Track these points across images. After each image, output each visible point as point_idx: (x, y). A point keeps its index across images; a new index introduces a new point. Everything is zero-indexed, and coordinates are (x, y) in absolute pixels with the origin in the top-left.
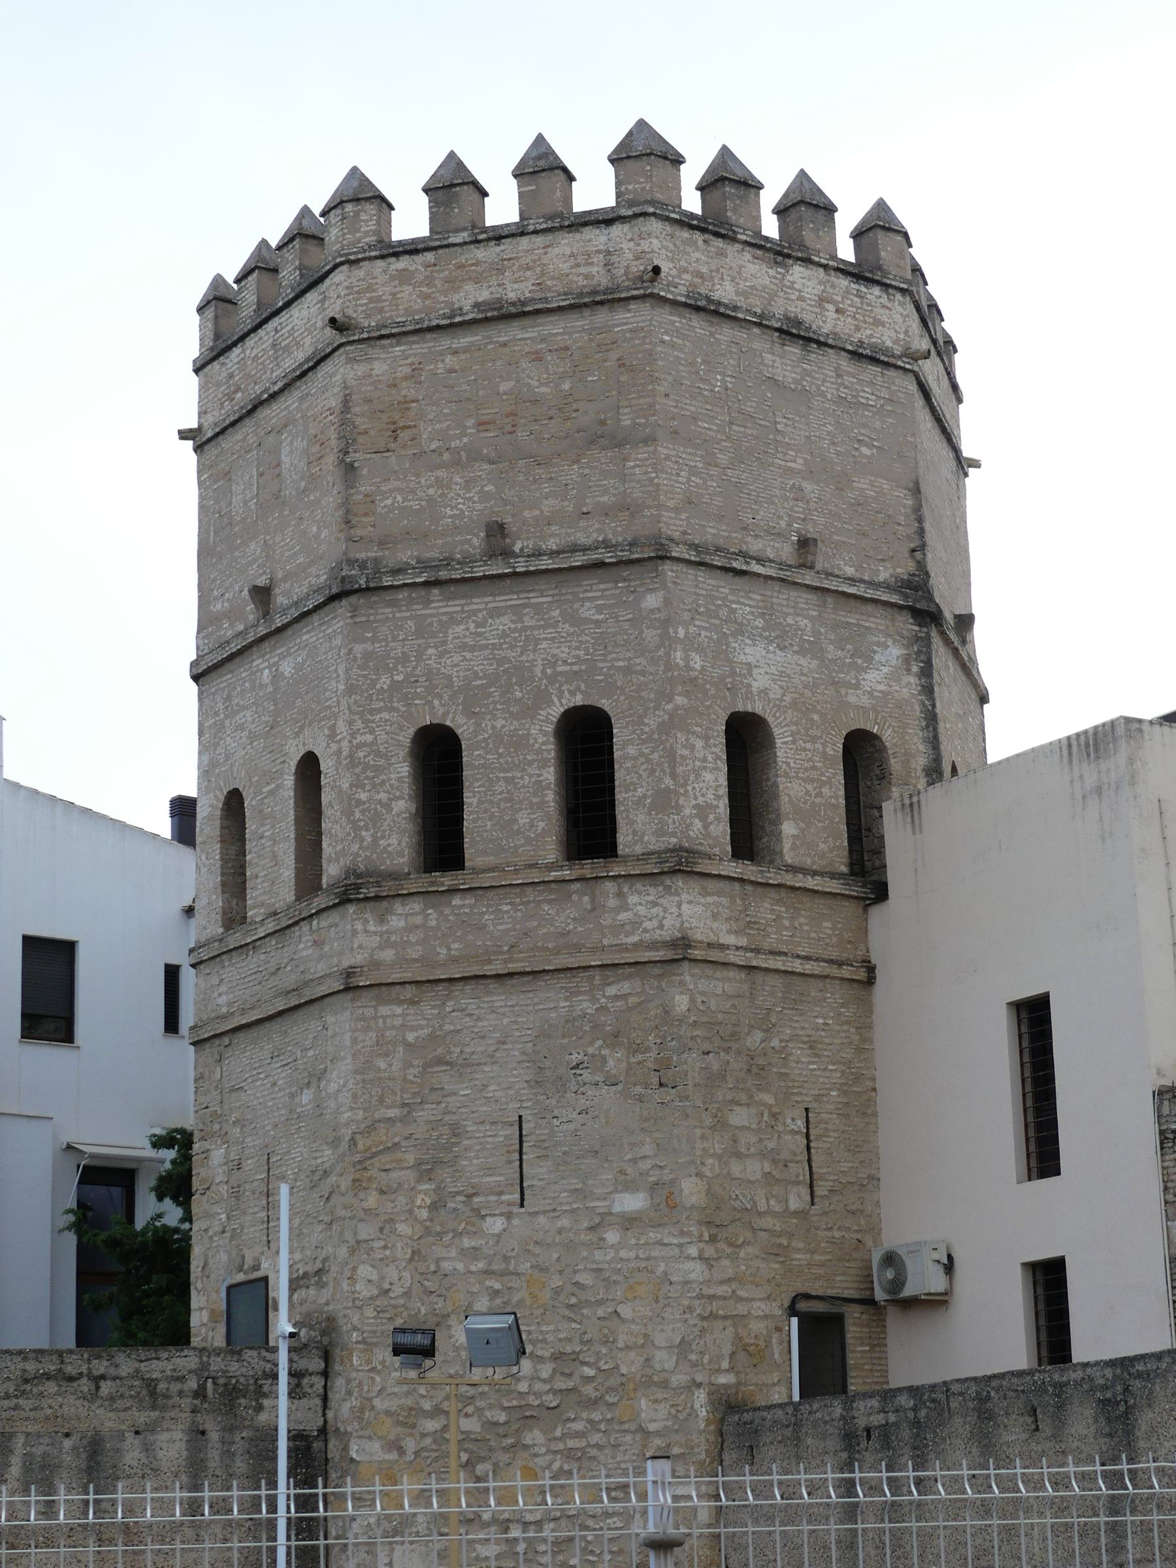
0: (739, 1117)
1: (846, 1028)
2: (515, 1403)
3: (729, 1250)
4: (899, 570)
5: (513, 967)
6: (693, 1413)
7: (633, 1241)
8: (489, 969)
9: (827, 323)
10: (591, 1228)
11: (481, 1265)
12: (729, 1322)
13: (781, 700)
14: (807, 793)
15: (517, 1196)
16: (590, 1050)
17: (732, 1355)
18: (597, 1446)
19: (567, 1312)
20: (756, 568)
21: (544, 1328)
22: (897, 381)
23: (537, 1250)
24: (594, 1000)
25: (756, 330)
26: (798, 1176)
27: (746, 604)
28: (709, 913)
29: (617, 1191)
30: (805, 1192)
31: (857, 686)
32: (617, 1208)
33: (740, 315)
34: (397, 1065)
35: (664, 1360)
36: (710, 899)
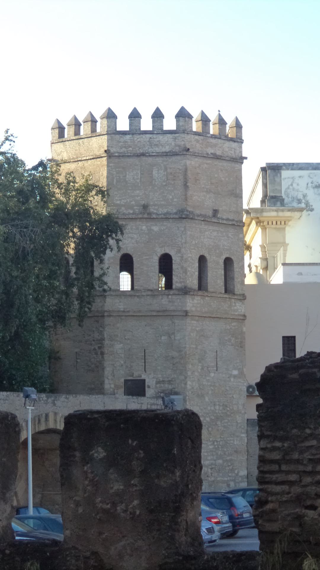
5: (217, 316)
11: (209, 384)
32: (233, 374)
35: (241, 407)
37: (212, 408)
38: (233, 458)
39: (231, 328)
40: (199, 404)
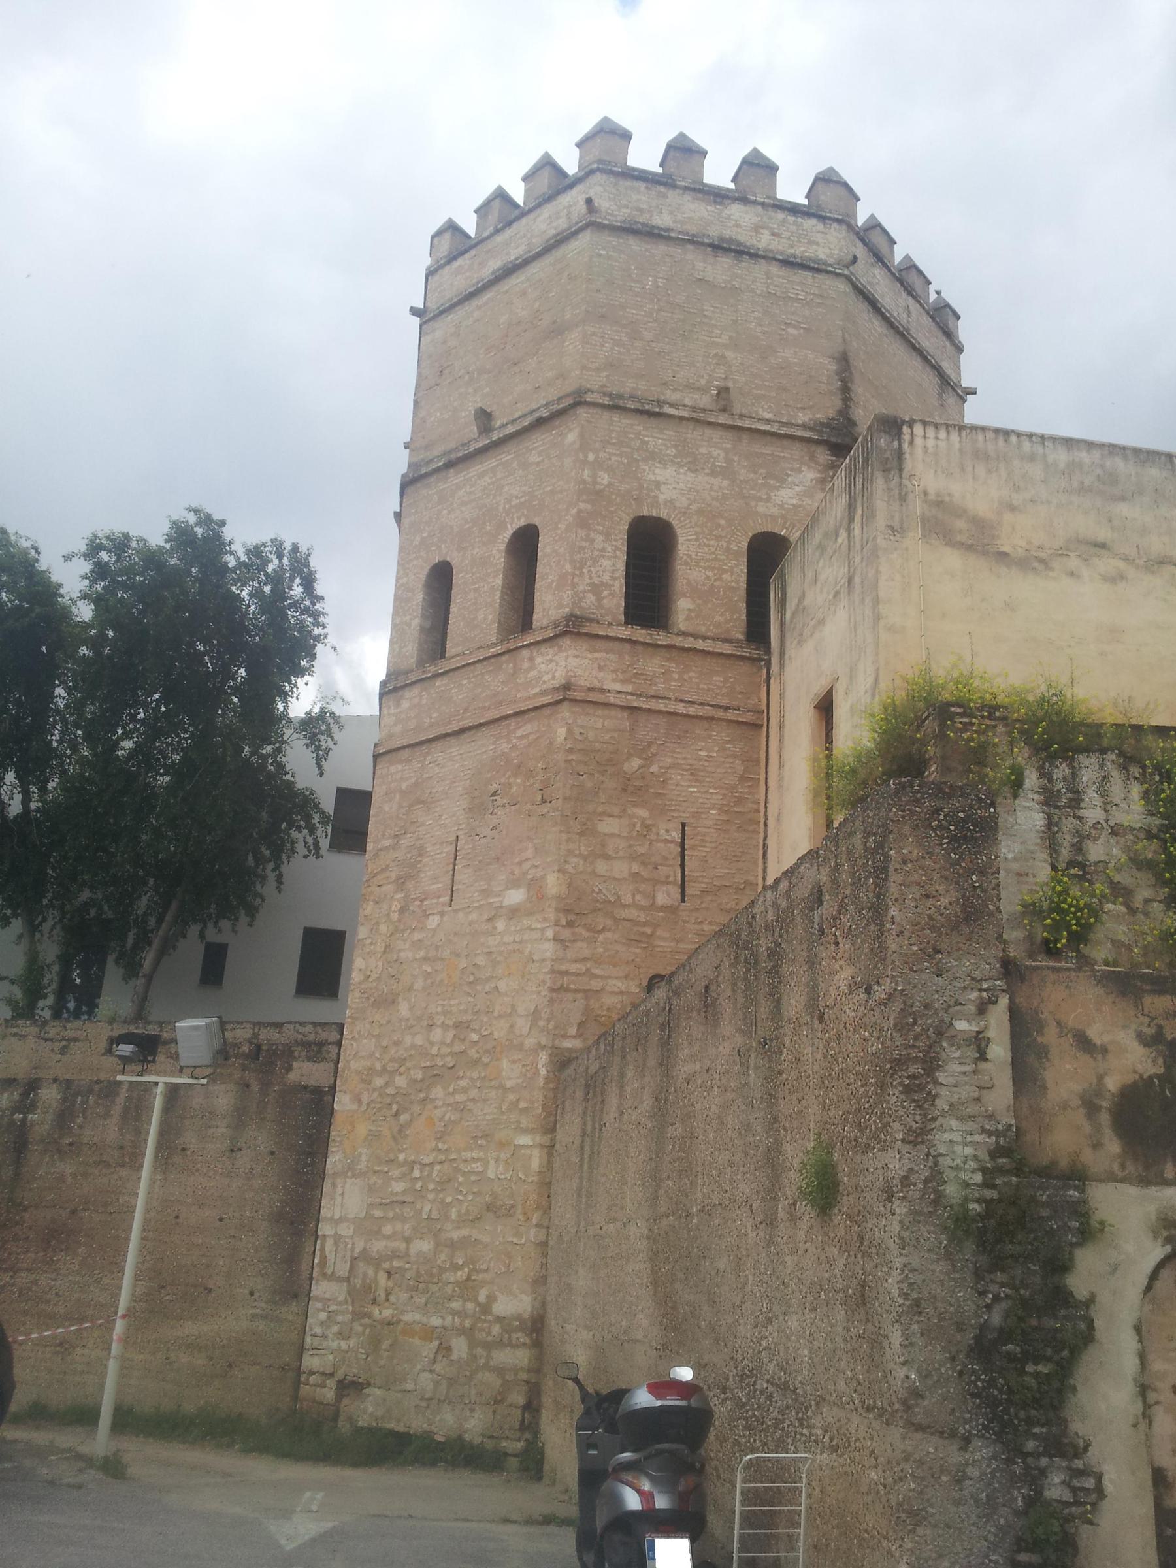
0: (608, 826)
1: (730, 760)
2: (428, 1064)
3: (586, 934)
4: (818, 416)
6: (537, 1072)
7: (513, 928)
9: (764, 241)
10: (490, 920)
11: (422, 954)
12: (580, 995)
13: (688, 508)
14: (708, 578)
15: (448, 898)
16: (503, 781)
17: (581, 1025)
18: (473, 1099)
20: (667, 410)
21: (452, 1002)
22: (828, 282)
24: (509, 741)
25: (690, 247)
26: (668, 877)
27: (657, 438)
28: (595, 665)
29: (507, 889)
30: (675, 892)
31: (768, 500)
32: (506, 903)
33: (673, 235)
35: (522, 1025)
36: (596, 655)
37: (419, 1040)
38: (475, 1235)
39: (514, 747)
40: (377, 1032)
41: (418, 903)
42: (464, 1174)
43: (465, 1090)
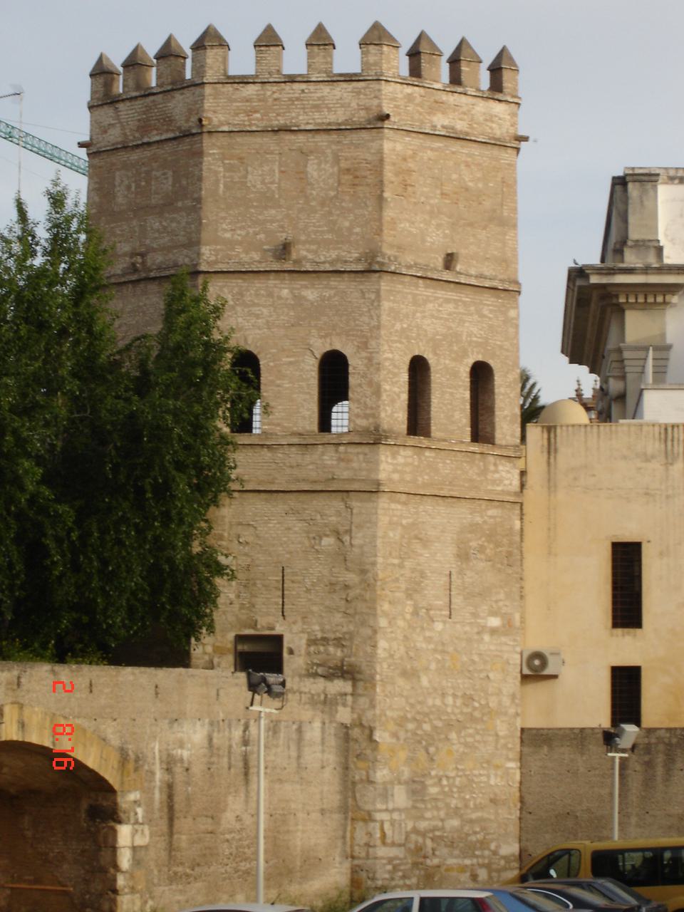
8: (442, 493)
10: (478, 633)
11: (432, 646)
16: (480, 543)
18: (478, 742)
19: (467, 674)
23: (456, 641)
24: (482, 517)
34: (397, 537)
35: (506, 701)
37: (438, 702)
38: (486, 815)
39: (485, 522)
40: (405, 693)
41: (424, 610)
42: (476, 783)
43: (470, 735)
